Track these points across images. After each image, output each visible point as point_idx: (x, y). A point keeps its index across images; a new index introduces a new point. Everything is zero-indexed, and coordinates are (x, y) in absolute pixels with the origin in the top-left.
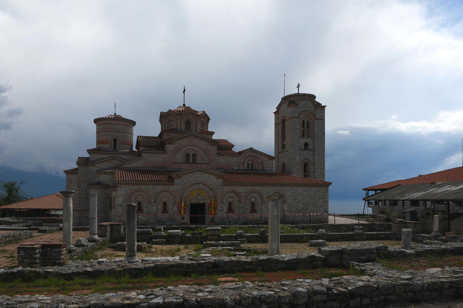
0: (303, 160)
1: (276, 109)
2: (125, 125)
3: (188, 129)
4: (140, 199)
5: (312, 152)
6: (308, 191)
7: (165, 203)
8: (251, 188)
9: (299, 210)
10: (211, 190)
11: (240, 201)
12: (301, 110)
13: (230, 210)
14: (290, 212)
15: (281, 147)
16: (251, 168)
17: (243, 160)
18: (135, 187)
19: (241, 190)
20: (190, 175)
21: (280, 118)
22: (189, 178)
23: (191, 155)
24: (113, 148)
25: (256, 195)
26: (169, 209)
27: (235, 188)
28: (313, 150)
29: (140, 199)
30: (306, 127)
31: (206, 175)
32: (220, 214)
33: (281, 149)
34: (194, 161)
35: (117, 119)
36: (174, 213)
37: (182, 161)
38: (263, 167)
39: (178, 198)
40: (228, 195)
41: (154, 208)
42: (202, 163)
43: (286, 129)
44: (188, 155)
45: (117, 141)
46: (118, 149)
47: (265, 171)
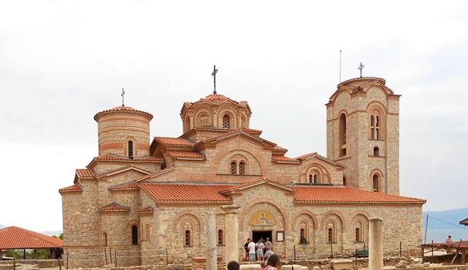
0: (373, 170)
4: (188, 226)
5: (382, 159)
8: (329, 209)
11: (314, 227)
13: (303, 241)
15: (338, 152)
18: (182, 209)
19: (318, 212)
20: (253, 190)
21: (337, 112)
23: (238, 164)
24: (127, 155)
25: (335, 218)
27: (309, 208)
29: (188, 226)
31: (273, 191)
32: (290, 245)
33: (338, 155)
35: (124, 111)
40: (300, 219)
44: (234, 163)
45: (134, 145)
46: (134, 155)
47: (332, 185)
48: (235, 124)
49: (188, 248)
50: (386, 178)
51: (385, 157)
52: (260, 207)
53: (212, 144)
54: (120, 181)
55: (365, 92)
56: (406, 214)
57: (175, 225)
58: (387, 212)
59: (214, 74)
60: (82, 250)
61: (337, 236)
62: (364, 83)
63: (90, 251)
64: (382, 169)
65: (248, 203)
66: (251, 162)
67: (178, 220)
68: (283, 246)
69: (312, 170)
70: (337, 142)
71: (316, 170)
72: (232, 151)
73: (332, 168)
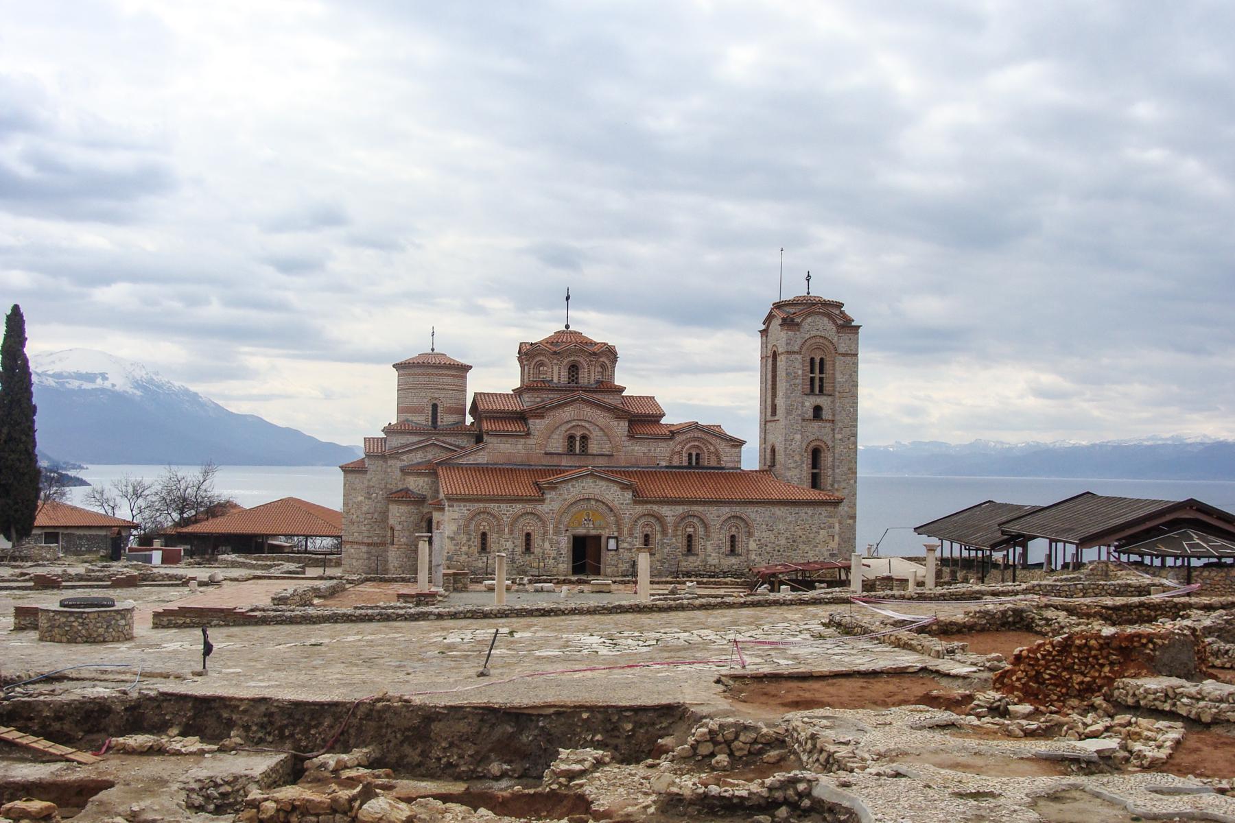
1: (764, 323)
2: (452, 375)
3: (573, 381)
4: (484, 526)
5: (828, 425)
7: (528, 535)
8: (686, 508)
9: (779, 551)
10: (611, 510)
11: (664, 532)
12: (807, 336)
14: (760, 555)
16: (697, 463)
17: (678, 448)
19: (669, 513)
21: (770, 347)
22: (572, 489)
23: (578, 439)
24: (430, 423)
25: (695, 520)
26: (536, 545)
27: (655, 508)
28: (833, 421)
29: (484, 527)
30: (817, 371)
31: (603, 483)
34: (584, 451)
36: (543, 553)
37: (560, 450)
38: (719, 461)
39: (552, 526)
41: (509, 545)
42: (599, 453)
43: (778, 373)
44: (571, 438)
45: (439, 408)
46: (439, 423)
47: (723, 468)
48: (588, 376)
49: (483, 555)
50: (834, 453)
52: (584, 505)
53: (539, 413)
54: (418, 457)
55: (798, 324)
56: (811, 517)
57: (467, 525)
59: (568, 298)
60: (364, 549)
61: (699, 545)
62: (802, 308)
63: (374, 550)
64: (828, 439)
66: (595, 434)
67: (472, 519)
68: (616, 558)
69: (689, 449)
70: (769, 392)
71: (698, 447)
72: (570, 421)
73: (724, 444)
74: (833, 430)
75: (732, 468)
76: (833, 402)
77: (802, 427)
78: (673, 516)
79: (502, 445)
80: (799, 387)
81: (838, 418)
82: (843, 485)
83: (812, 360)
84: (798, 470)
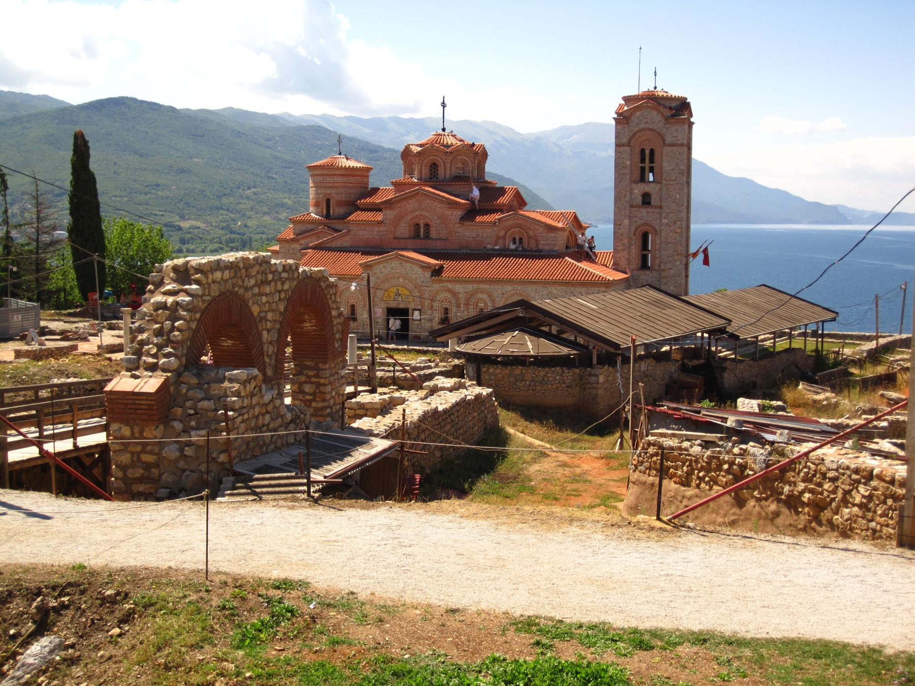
2: (342, 175)
3: (434, 176)
5: (657, 210)
6: (572, 292)
7: (353, 306)
8: (476, 286)
11: (458, 306)
12: (636, 129)
17: (502, 233)
27: (450, 285)
31: (408, 265)
34: (427, 236)
37: (407, 235)
38: (537, 245)
40: (442, 296)
47: (541, 251)
51: (661, 207)
58: (555, 291)
65: (378, 278)
73: (541, 230)
74: (661, 214)
75: (549, 251)
76: (661, 189)
77: (630, 213)
78: (465, 293)
79: (361, 233)
80: (628, 177)
81: (664, 204)
82: (669, 266)
83: (643, 151)
84: (625, 252)
